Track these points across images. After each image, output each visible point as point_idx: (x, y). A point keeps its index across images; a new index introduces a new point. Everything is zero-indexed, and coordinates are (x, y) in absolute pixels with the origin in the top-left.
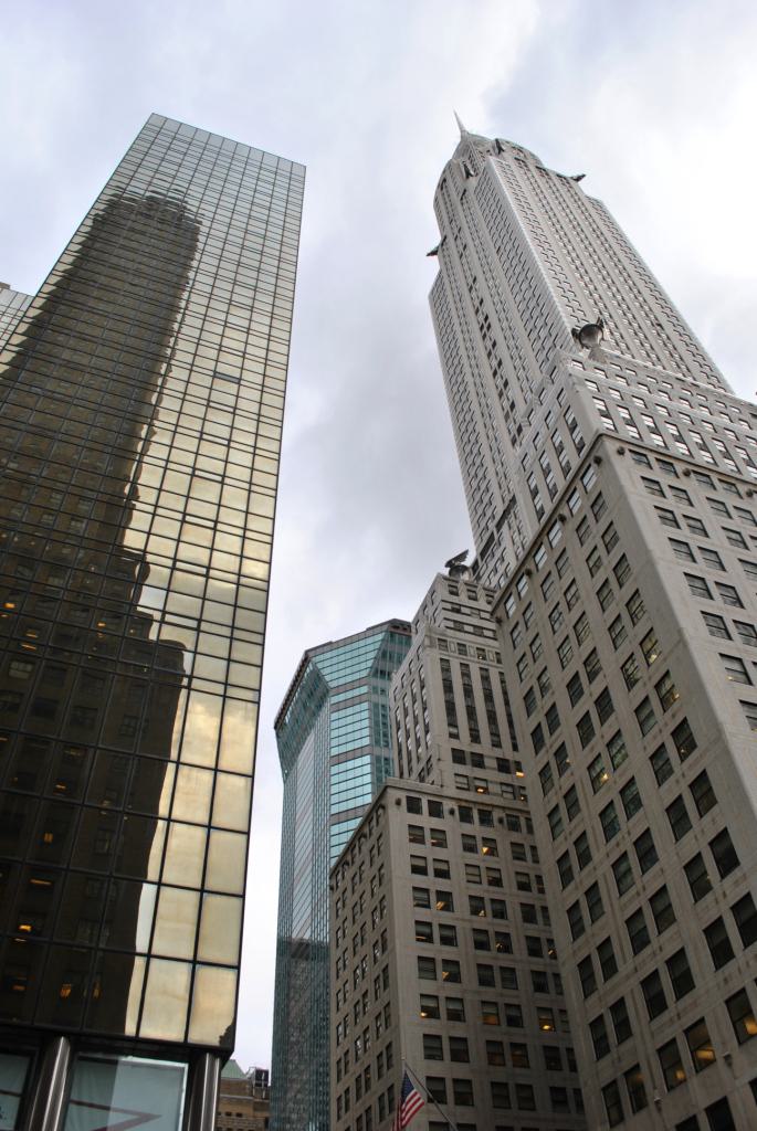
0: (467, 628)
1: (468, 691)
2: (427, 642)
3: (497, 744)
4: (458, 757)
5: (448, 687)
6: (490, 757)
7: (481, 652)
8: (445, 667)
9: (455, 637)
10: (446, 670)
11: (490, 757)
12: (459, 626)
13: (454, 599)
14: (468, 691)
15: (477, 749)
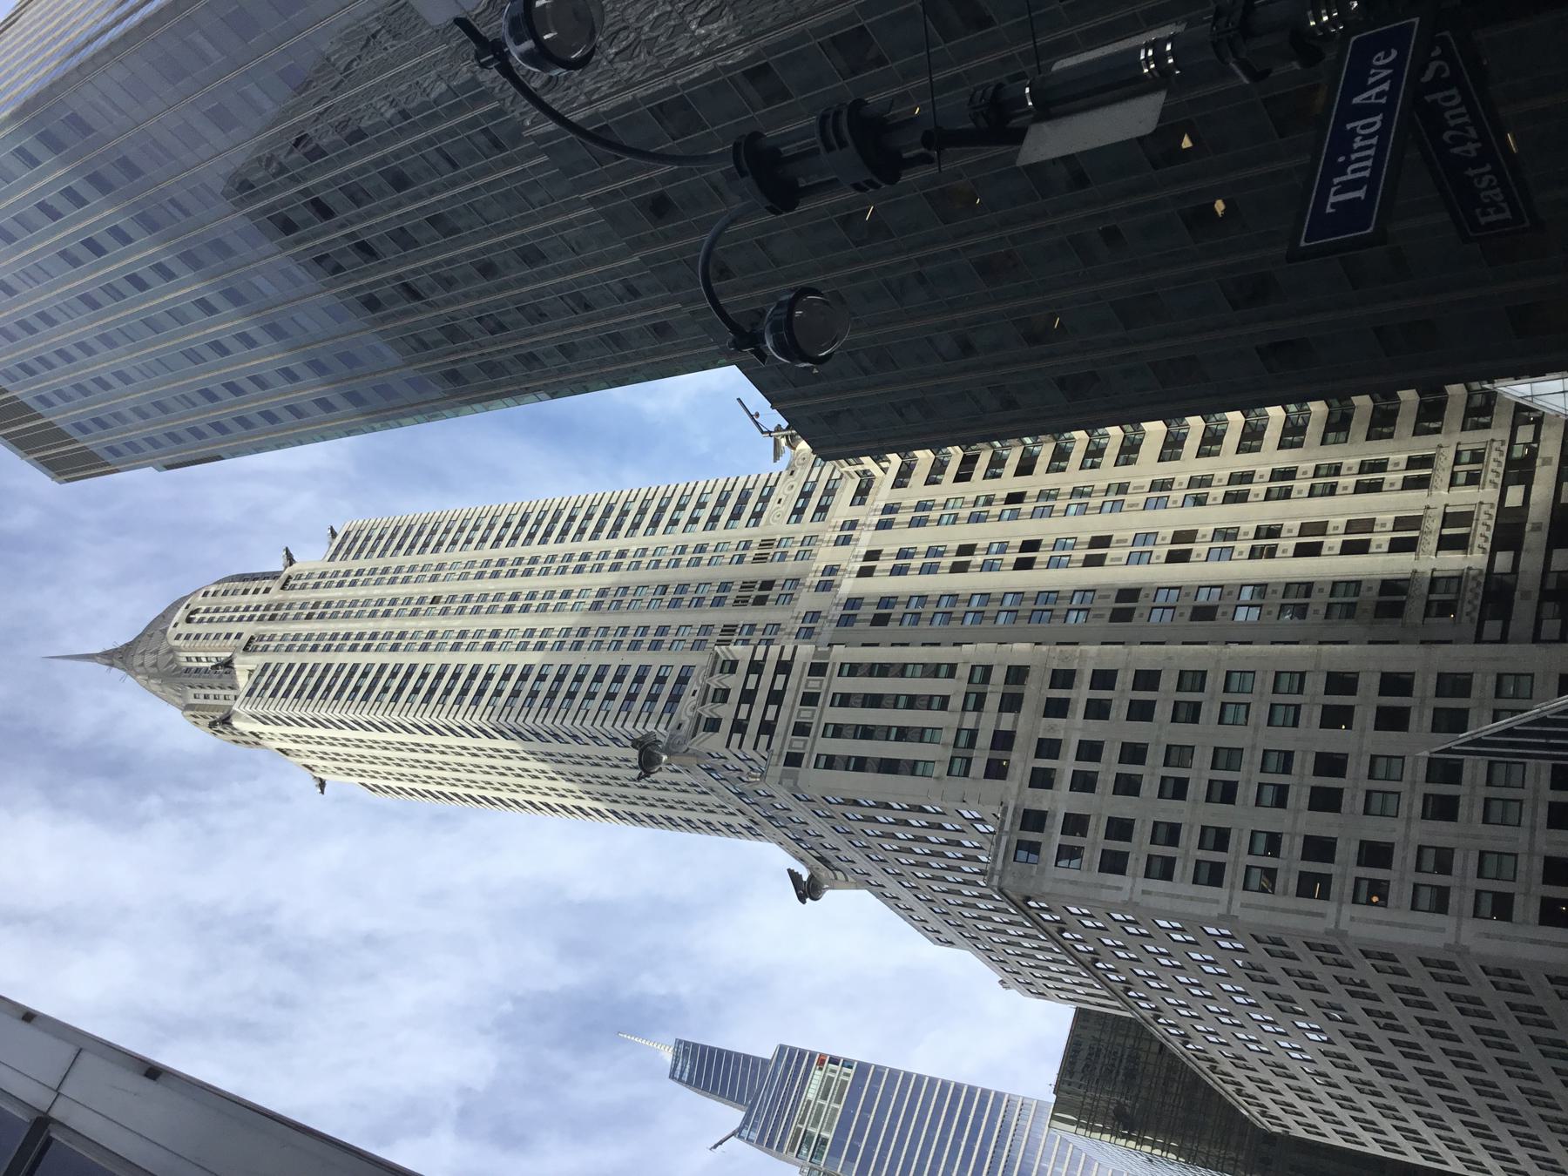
0: (770, 716)
1: (866, 732)
2: (790, 782)
3: (944, 702)
4: (960, 766)
5: (860, 764)
6: (962, 719)
7: (810, 699)
8: (830, 762)
9: (784, 740)
10: (830, 762)
11: (962, 719)
12: (767, 728)
13: (726, 726)
14: (866, 732)
15: (949, 737)
